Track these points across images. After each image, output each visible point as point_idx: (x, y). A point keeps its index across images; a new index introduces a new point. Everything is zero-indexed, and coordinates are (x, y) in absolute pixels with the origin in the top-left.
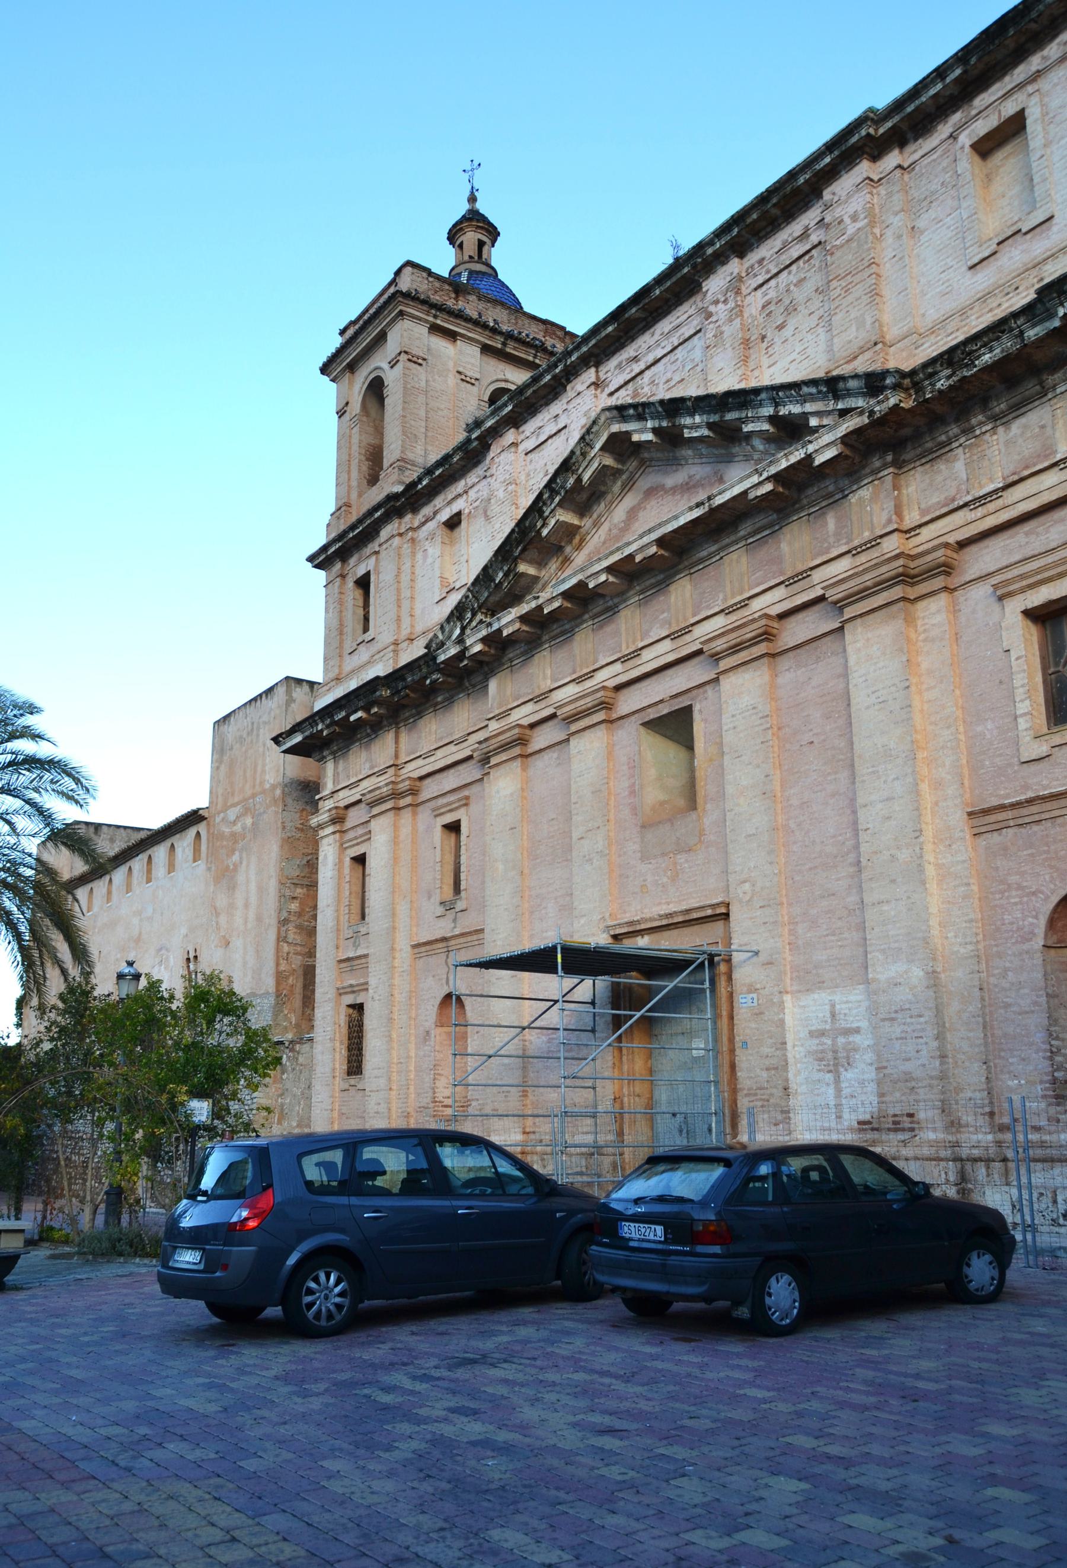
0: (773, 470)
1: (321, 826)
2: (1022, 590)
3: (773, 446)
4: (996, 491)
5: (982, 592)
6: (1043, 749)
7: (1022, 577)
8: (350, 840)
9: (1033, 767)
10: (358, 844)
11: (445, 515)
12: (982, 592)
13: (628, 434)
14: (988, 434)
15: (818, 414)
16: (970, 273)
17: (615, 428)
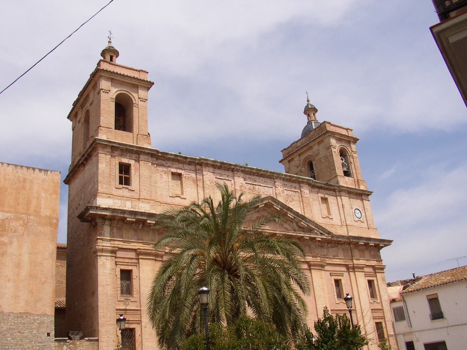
0: (310, 236)
1: (102, 251)
2: (334, 276)
3: (297, 227)
4: (332, 258)
5: (328, 273)
6: (338, 302)
7: (335, 274)
8: (120, 262)
9: (337, 304)
10: (128, 265)
11: (174, 170)
12: (328, 273)
13: (274, 205)
14: (329, 248)
15: (317, 230)
16: (322, 218)
17: (270, 201)
